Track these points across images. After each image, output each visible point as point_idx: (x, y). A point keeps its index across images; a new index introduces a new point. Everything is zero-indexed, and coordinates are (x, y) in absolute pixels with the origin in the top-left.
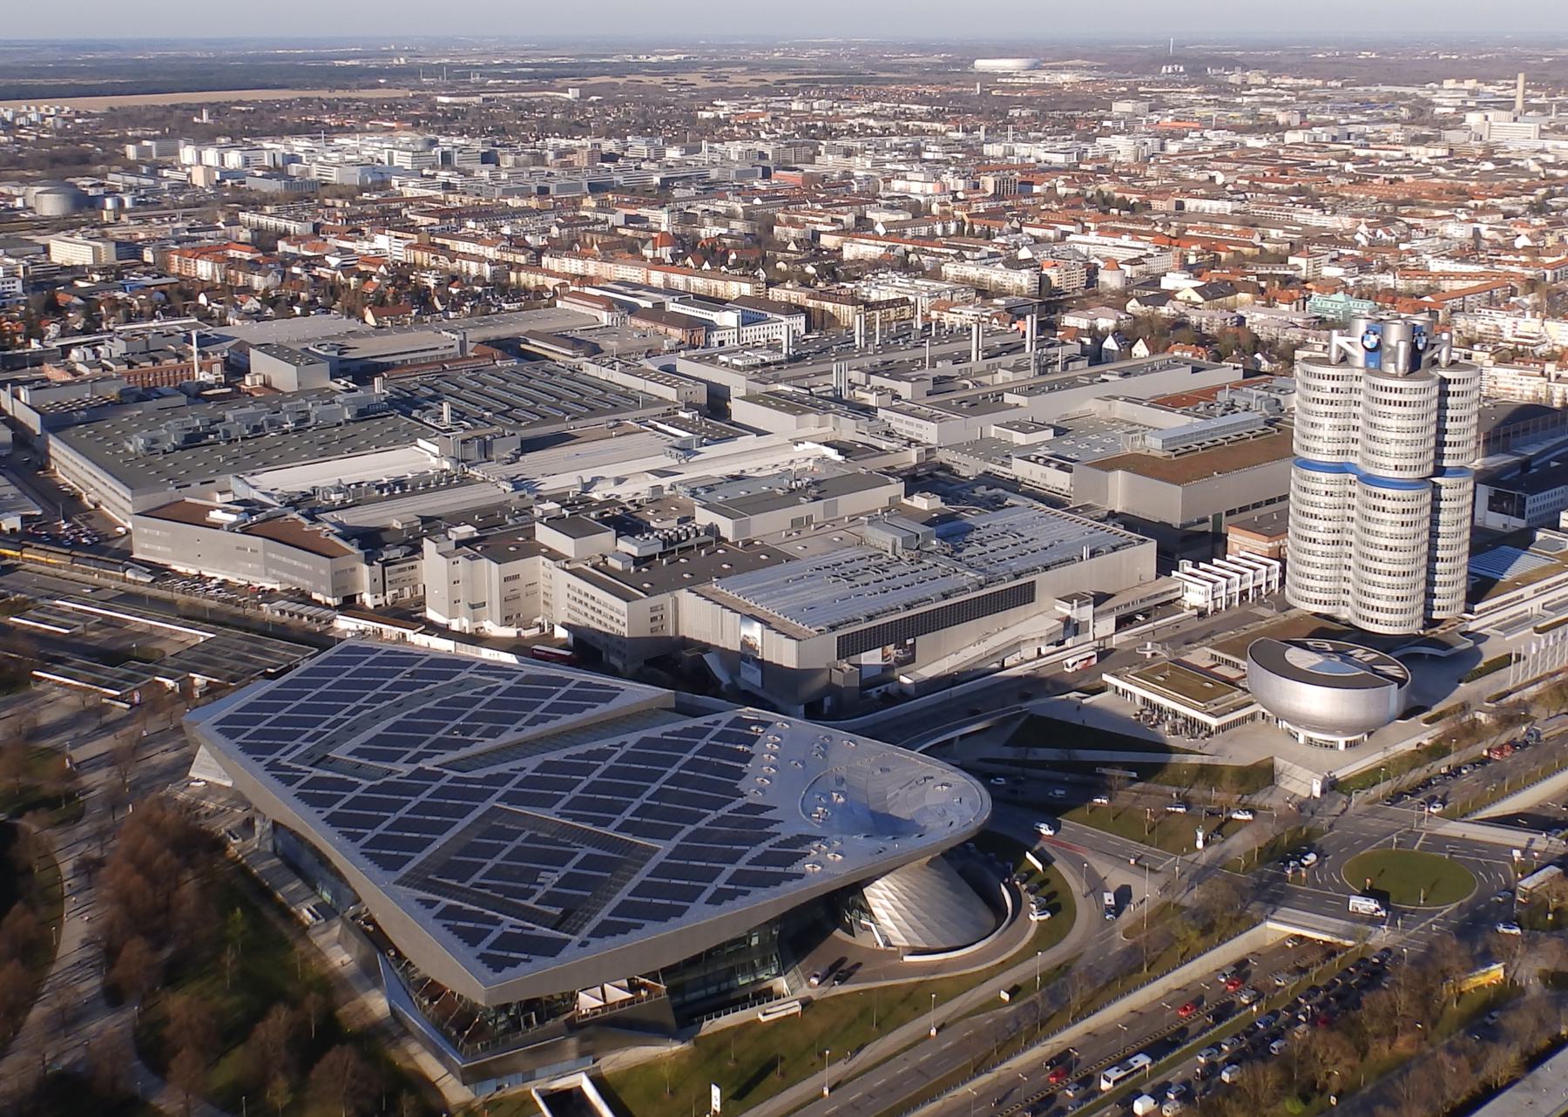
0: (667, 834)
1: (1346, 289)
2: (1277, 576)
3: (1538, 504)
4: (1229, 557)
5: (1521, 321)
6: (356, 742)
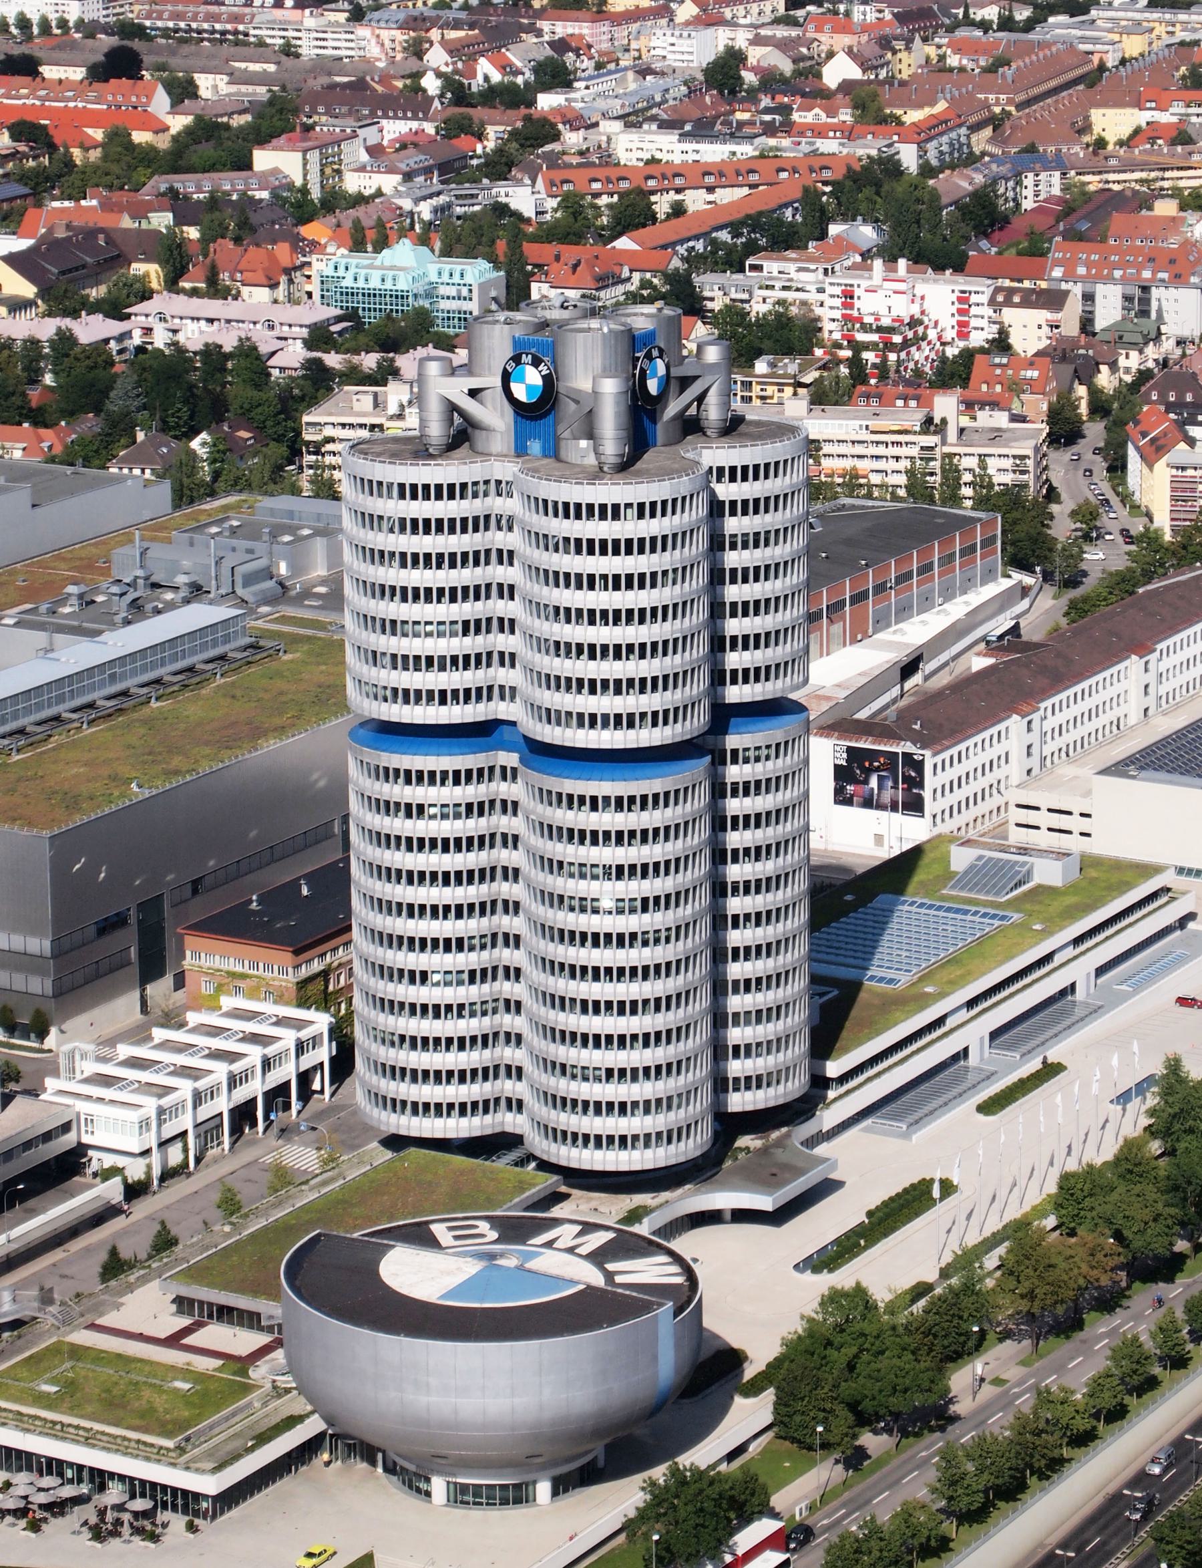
1: (406, 226)
2: (323, 1054)
3: (952, 773)
4: (193, 1018)
5: (860, 284)
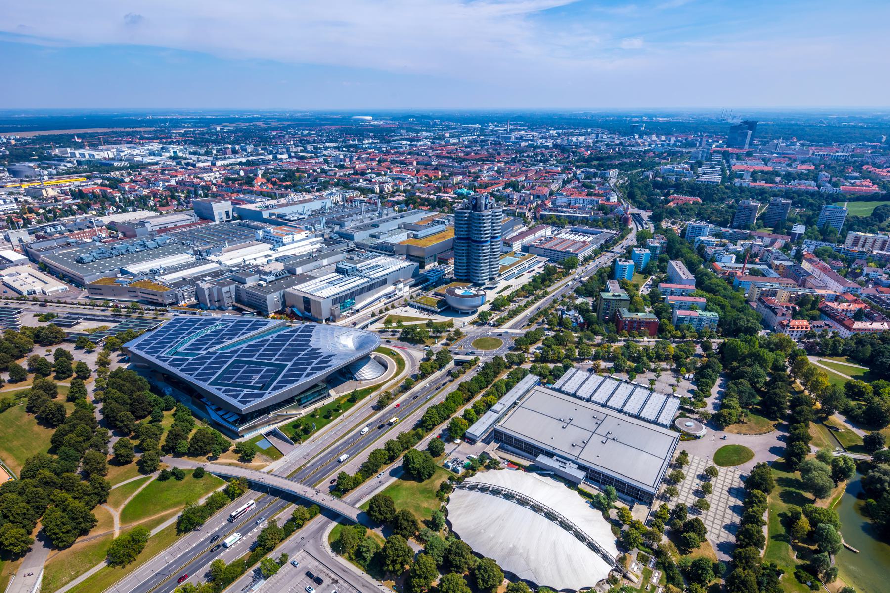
0: (290, 360)
6: (185, 347)
